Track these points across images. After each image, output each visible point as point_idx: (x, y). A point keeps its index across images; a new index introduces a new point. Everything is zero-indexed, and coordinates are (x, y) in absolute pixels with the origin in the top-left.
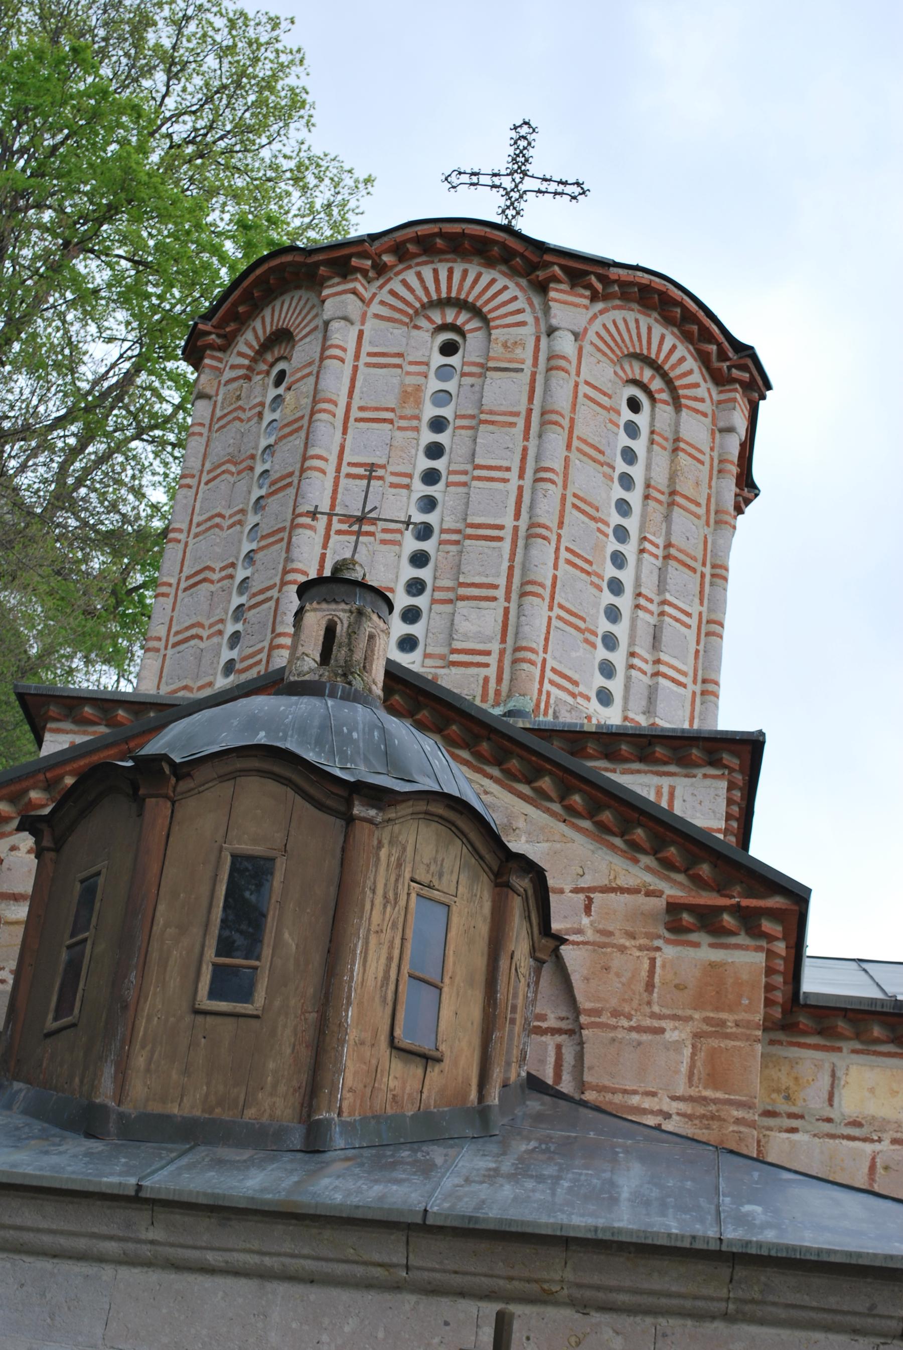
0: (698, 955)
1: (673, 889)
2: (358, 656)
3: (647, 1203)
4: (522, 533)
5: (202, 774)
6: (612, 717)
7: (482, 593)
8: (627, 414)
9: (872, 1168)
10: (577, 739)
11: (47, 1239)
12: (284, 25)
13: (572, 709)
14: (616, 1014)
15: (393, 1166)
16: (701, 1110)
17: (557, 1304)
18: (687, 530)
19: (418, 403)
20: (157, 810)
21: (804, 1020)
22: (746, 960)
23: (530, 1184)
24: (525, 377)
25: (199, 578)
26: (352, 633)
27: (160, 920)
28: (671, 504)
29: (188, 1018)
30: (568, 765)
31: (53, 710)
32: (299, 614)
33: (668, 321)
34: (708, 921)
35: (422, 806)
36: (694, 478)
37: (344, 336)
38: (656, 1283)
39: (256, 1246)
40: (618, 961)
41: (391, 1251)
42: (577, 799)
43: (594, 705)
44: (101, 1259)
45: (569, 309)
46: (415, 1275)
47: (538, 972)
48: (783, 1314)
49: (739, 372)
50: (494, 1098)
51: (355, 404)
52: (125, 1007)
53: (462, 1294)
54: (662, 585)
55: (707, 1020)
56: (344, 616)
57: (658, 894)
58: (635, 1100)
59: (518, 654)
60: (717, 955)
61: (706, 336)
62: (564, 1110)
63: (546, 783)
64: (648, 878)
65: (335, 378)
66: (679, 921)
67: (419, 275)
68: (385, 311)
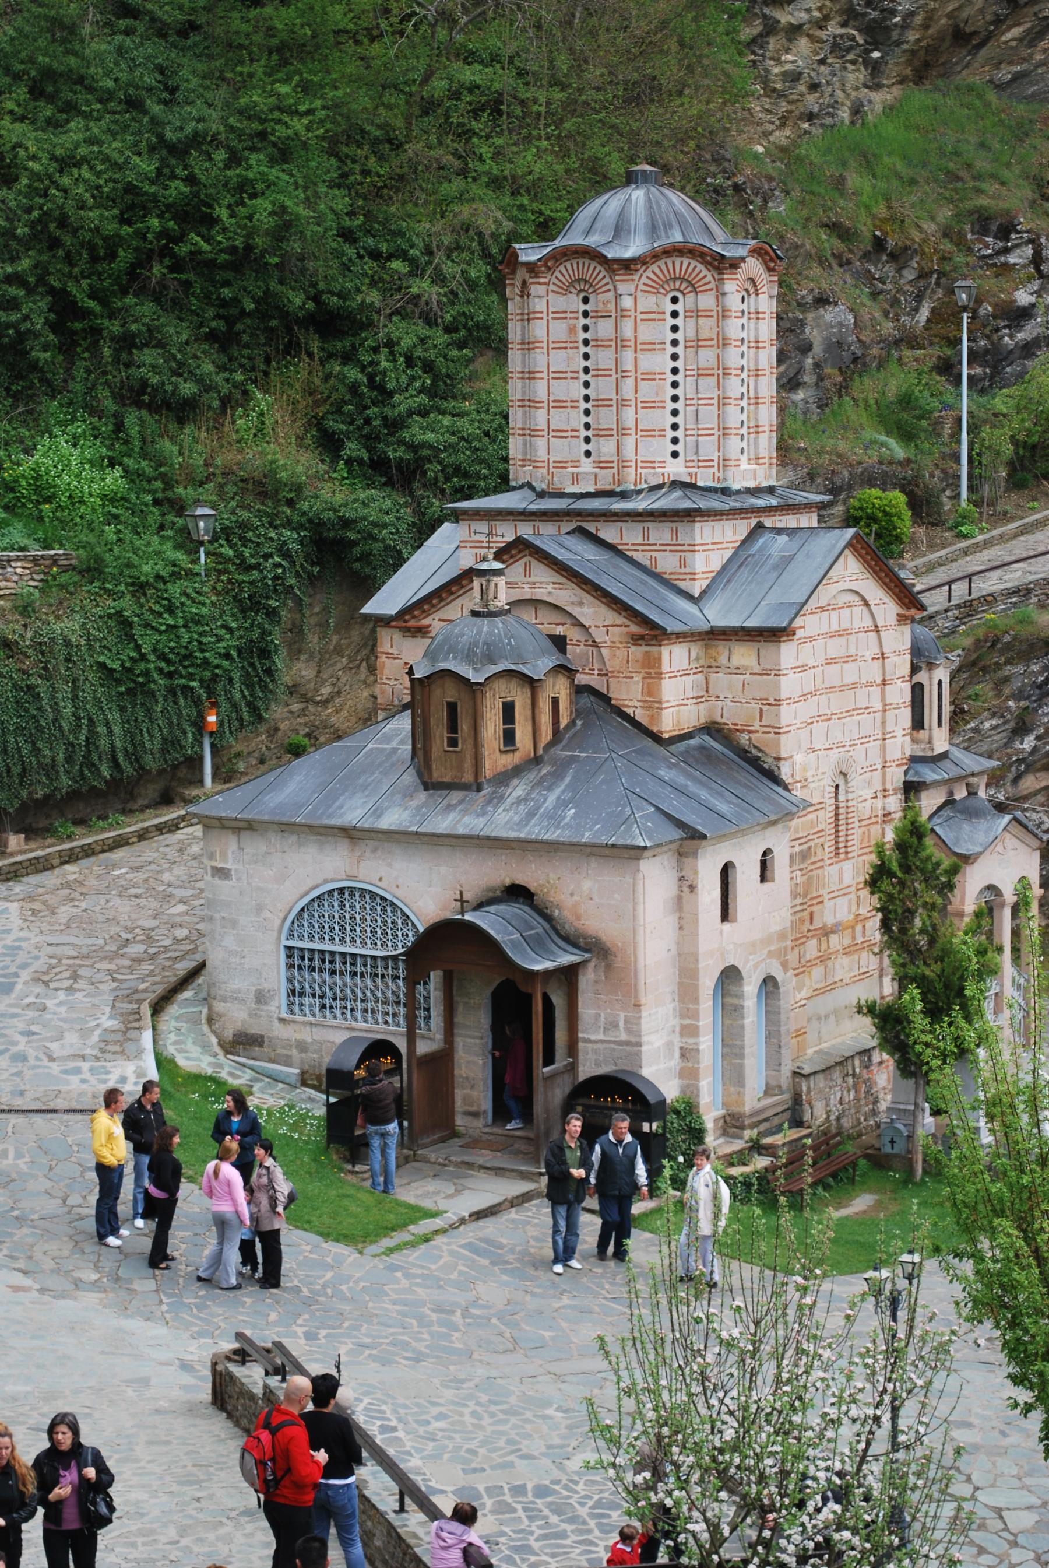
0: (637, 652)
59: (622, 464)
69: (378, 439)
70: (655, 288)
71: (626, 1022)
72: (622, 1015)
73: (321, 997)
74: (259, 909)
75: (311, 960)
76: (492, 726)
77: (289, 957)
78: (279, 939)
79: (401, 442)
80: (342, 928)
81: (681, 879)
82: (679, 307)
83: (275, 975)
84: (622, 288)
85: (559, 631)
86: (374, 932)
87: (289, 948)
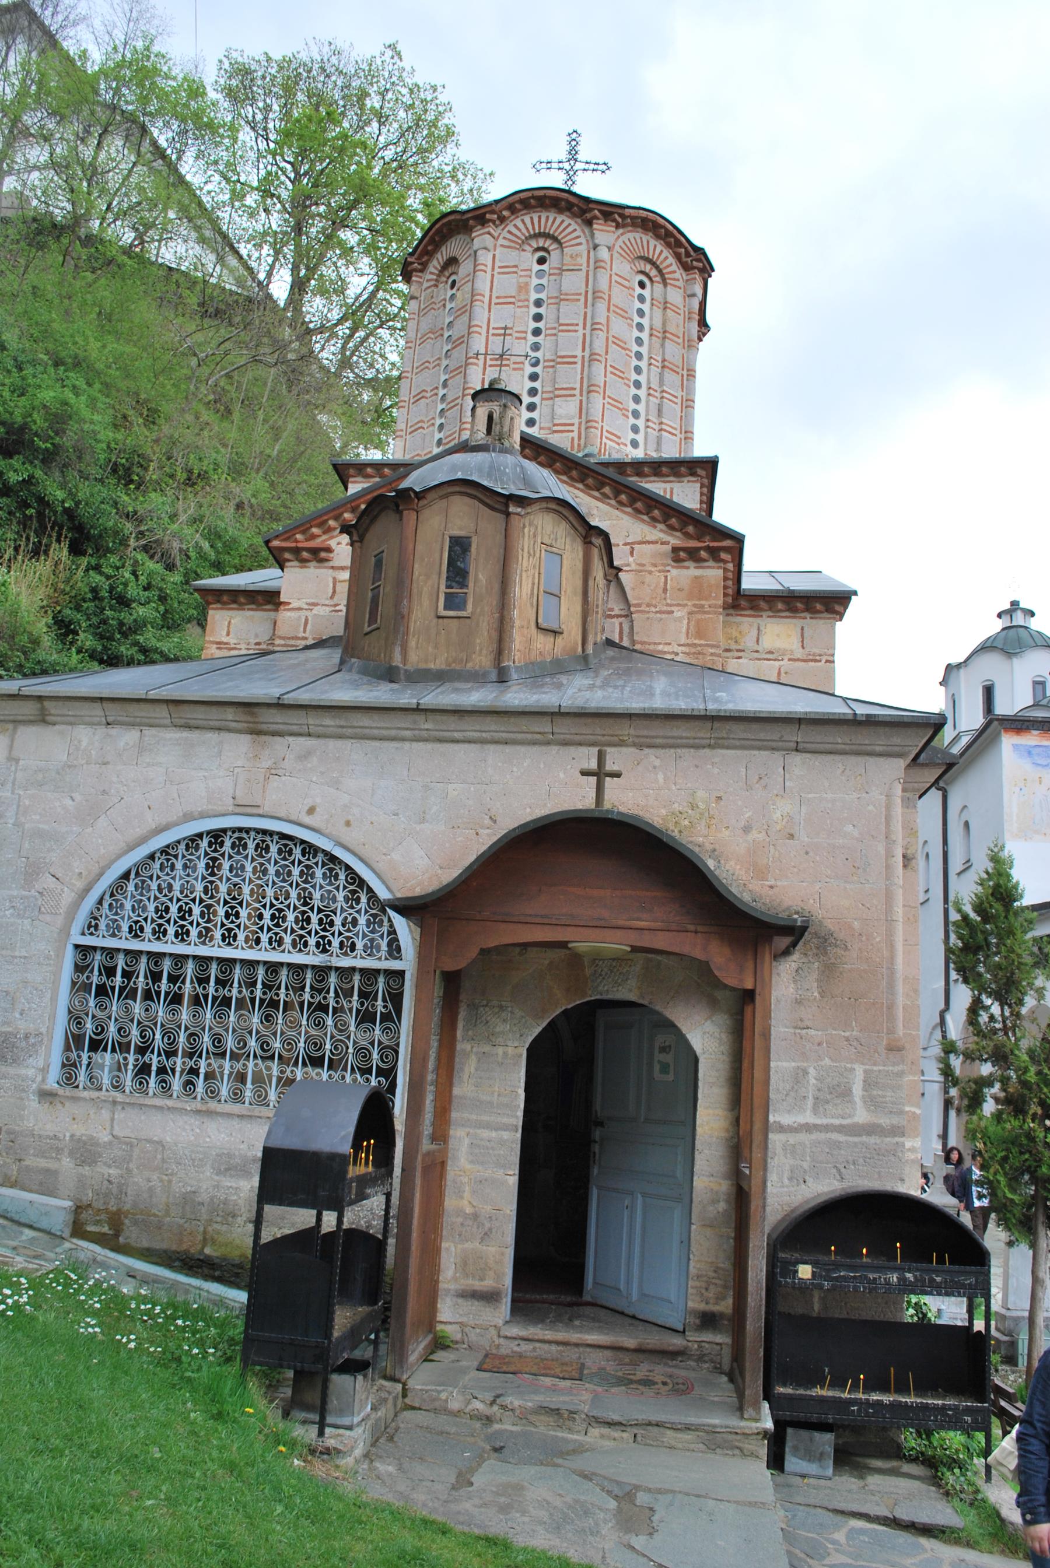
1: (675, 540)
2: (506, 429)
3: (669, 695)
4: (587, 359)
5: (430, 496)
6: (639, 454)
7: (567, 393)
8: (638, 290)
9: (779, 673)
10: (621, 466)
11: (376, 732)
12: (440, 89)
13: (618, 451)
14: (648, 605)
15: (542, 686)
16: (693, 650)
17: (627, 746)
18: (673, 352)
19: (527, 292)
20: (409, 516)
21: (743, 603)
22: (713, 574)
23: (611, 690)
24: (583, 274)
25: (419, 397)
26: (502, 417)
27: (416, 573)
28: (664, 338)
29: (435, 620)
30: (617, 480)
31: (352, 471)
32: (474, 409)
33: (658, 237)
34: (693, 555)
35: (544, 505)
36: (676, 322)
37: (485, 258)
38: (676, 733)
39: (478, 727)
40: (648, 578)
41: (544, 726)
42: (623, 497)
43: (630, 448)
44: (403, 739)
45: (605, 234)
46: (556, 737)
47: (608, 586)
48: (738, 743)
49: (696, 262)
50: (590, 650)
51: (494, 295)
52: (403, 617)
53: (580, 744)
54: (661, 382)
55: (695, 605)
56: (497, 408)
57: (667, 543)
58: (660, 647)
59: (588, 424)
60: (699, 572)
61: (678, 244)
62: (624, 653)
63: (607, 490)
64: (662, 535)
65: (483, 284)
66: (678, 556)
67: (523, 221)
68: (506, 243)
69: (111, 639)
71: (868, 1084)
72: (859, 1071)
73: (142, 1051)
74: (32, 872)
75: (126, 974)
77: (79, 969)
78: (66, 931)
79: (136, 643)
82: (646, 293)
83: (47, 1004)
86: (278, 918)
87: (83, 950)
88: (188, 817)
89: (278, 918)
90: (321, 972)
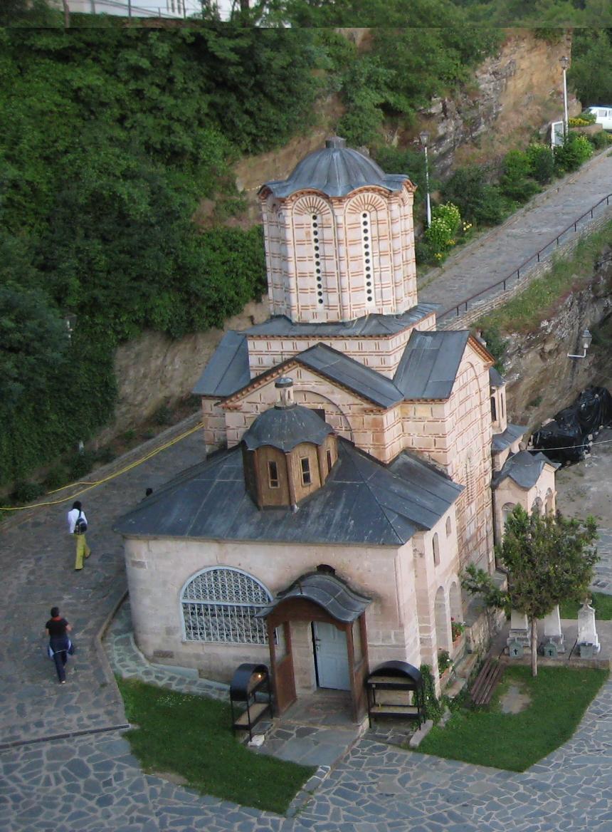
0: (369, 418)
1: (366, 406)
40: (357, 419)
59: (342, 307)
60: (375, 416)
70: (354, 211)
71: (395, 635)
76: (297, 473)
78: (178, 600)
80: (217, 591)
81: (415, 550)
82: (367, 219)
83: (179, 620)
84: (337, 212)
85: (320, 407)
86: (237, 592)
88: (205, 567)
89: (237, 592)
90: (251, 607)
